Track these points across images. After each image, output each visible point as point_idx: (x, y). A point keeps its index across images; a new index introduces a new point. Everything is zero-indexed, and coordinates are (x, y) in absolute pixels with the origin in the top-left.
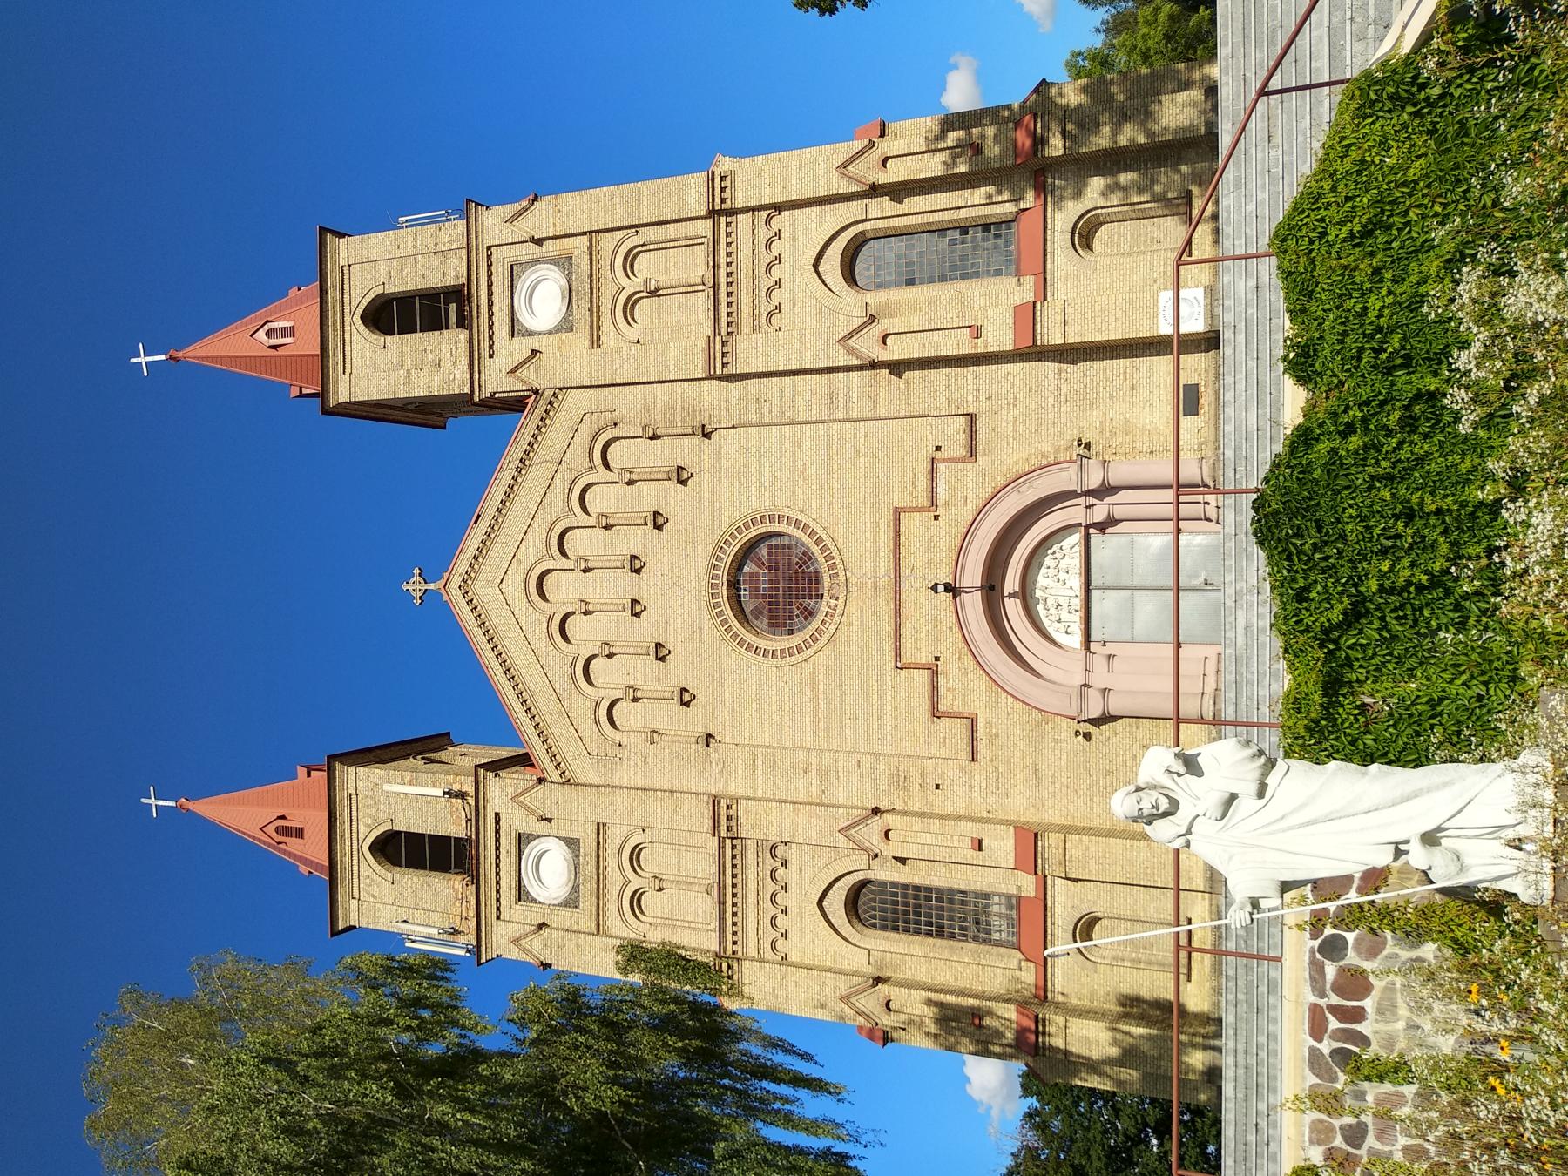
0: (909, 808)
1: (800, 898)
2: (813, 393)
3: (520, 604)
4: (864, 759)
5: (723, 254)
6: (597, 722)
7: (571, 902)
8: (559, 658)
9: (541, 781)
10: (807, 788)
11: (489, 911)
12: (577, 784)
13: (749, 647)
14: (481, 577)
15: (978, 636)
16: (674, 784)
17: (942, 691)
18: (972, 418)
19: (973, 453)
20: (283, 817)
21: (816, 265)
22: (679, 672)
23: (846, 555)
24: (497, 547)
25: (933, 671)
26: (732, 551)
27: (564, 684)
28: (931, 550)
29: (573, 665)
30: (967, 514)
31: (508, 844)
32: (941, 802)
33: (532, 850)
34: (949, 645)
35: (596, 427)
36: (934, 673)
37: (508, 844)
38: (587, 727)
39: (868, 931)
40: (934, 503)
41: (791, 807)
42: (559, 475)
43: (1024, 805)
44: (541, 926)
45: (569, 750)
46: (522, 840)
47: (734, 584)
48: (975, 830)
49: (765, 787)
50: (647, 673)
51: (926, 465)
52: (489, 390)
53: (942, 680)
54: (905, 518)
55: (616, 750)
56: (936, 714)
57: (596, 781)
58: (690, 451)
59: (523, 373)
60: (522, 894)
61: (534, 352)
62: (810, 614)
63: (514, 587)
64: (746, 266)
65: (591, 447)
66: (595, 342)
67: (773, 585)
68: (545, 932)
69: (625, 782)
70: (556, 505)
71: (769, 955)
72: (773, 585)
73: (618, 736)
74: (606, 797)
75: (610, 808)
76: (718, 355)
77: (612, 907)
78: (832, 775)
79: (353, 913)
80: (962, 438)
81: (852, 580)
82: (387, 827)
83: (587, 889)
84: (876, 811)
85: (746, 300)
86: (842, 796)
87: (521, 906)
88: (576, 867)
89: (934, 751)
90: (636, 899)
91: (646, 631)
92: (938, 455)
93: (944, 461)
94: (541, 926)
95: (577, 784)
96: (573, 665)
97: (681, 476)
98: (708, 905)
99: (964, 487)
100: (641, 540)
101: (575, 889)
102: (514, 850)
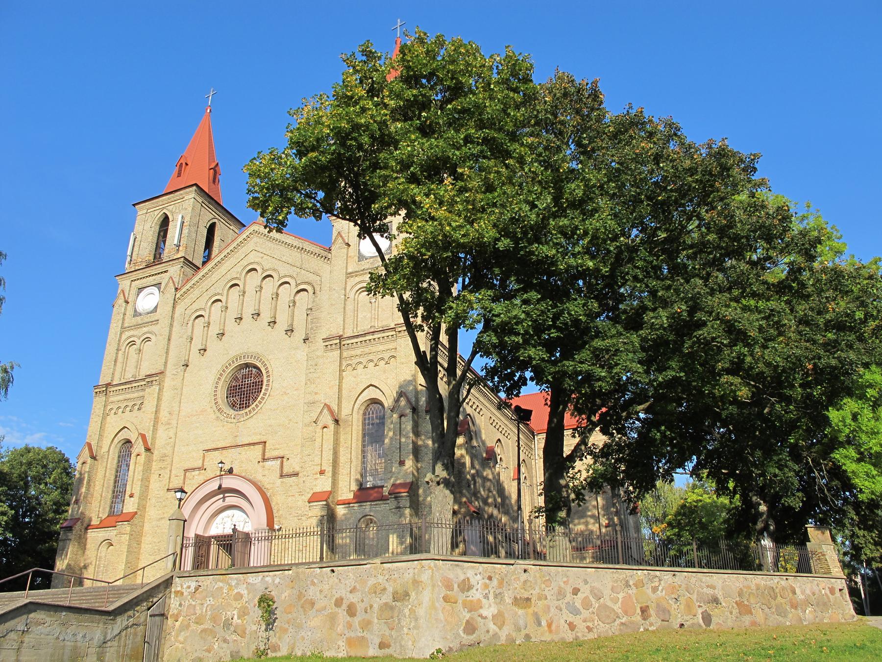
0: (154, 463)
1: (127, 418)
2: (316, 393)
3: (244, 262)
4: (172, 440)
5: (379, 336)
6: (196, 311)
7: (136, 314)
8: (220, 288)
9: (176, 289)
10: (164, 415)
11: (134, 276)
12: (174, 307)
13: (219, 379)
14: (258, 240)
15: (206, 488)
16: (171, 353)
17: (193, 473)
18: (296, 474)
19: (282, 476)
20: (187, 164)
21: (371, 385)
22: (214, 346)
23: (250, 420)
24: (270, 244)
25: (202, 468)
26: (259, 365)
27: (212, 291)
28: (245, 461)
29: (219, 294)
30: (258, 478)
31: (157, 279)
32: (154, 478)
33: (155, 290)
34: (210, 474)
35: (314, 284)
36: (199, 469)
37: (157, 279)
38: (196, 306)
39: (117, 451)
40: (264, 460)
41: (154, 410)
42: (295, 268)
43: (152, 512)
44: (127, 302)
45: (188, 301)
46: (158, 285)
47: (247, 365)
48: (137, 495)
49: (167, 395)
50: (214, 330)
51: (282, 455)
52: (335, 224)
53: (197, 472)
54: (260, 447)
55: (186, 322)
56: (186, 471)
57: (176, 316)
58: (300, 334)
59: (340, 240)
60: (141, 289)
61: (348, 245)
62: (233, 406)
63: (252, 257)
64: (374, 349)
65: (306, 283)
66: (349, 275)
67: (245, 387)
68: (124, 304)
69: (174, 329)
70: (284, 270)
71: (109, 407)
72: (245, 387)
73: (191, 323)
74: (167, 322)
75: (165, 322)
76: (331, 343)
77: (131, 333)
78: (167, 426)
79: (142, 209)
80: (291, 471)
81: (240, 424)
82: (171, 218)
83: (139, 320)
84: (148, 449)
85: (358, 352)
86: (161, 433)
87: (134, 291)
88: (148, 313)
89: (173, 472)
90: (133, 343)
91: (231, 325)
92: (285, 460)
93: (282, 463)
94: (127, 302)
95: (174, 307)
96: (219, 294)
97: (290, 331)
98: (129, 377)
99: (268, 475)
100: (266, 317)
101: (140, 314)
102: (155, 282)
